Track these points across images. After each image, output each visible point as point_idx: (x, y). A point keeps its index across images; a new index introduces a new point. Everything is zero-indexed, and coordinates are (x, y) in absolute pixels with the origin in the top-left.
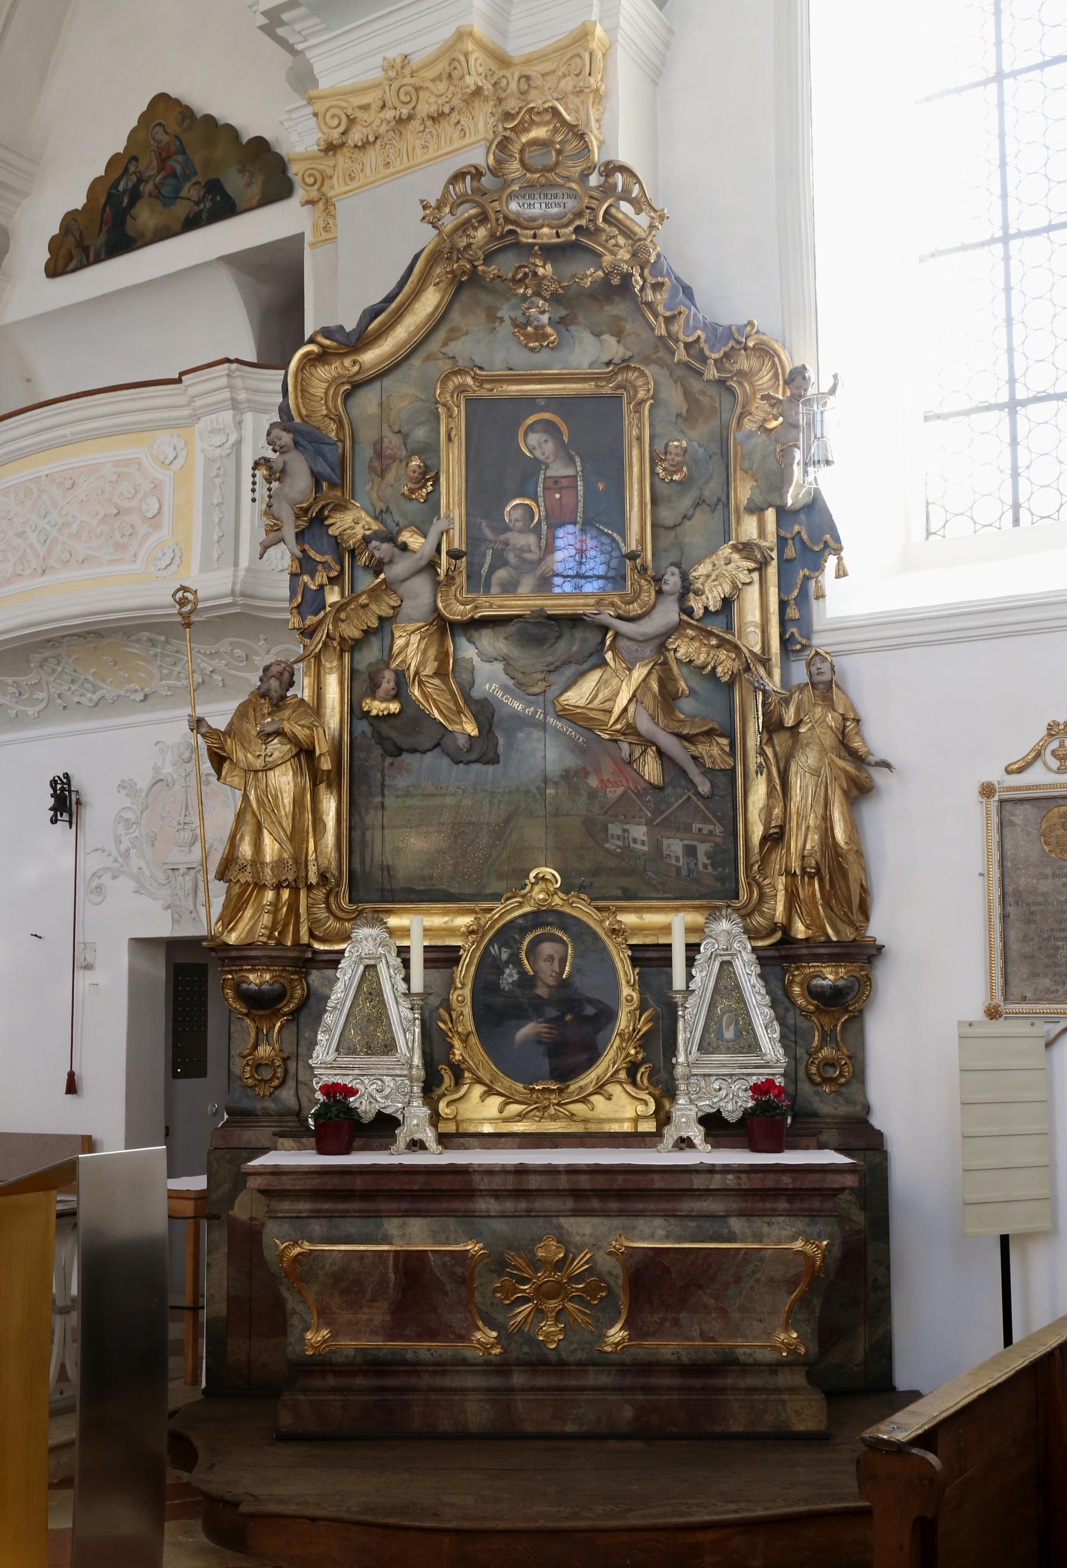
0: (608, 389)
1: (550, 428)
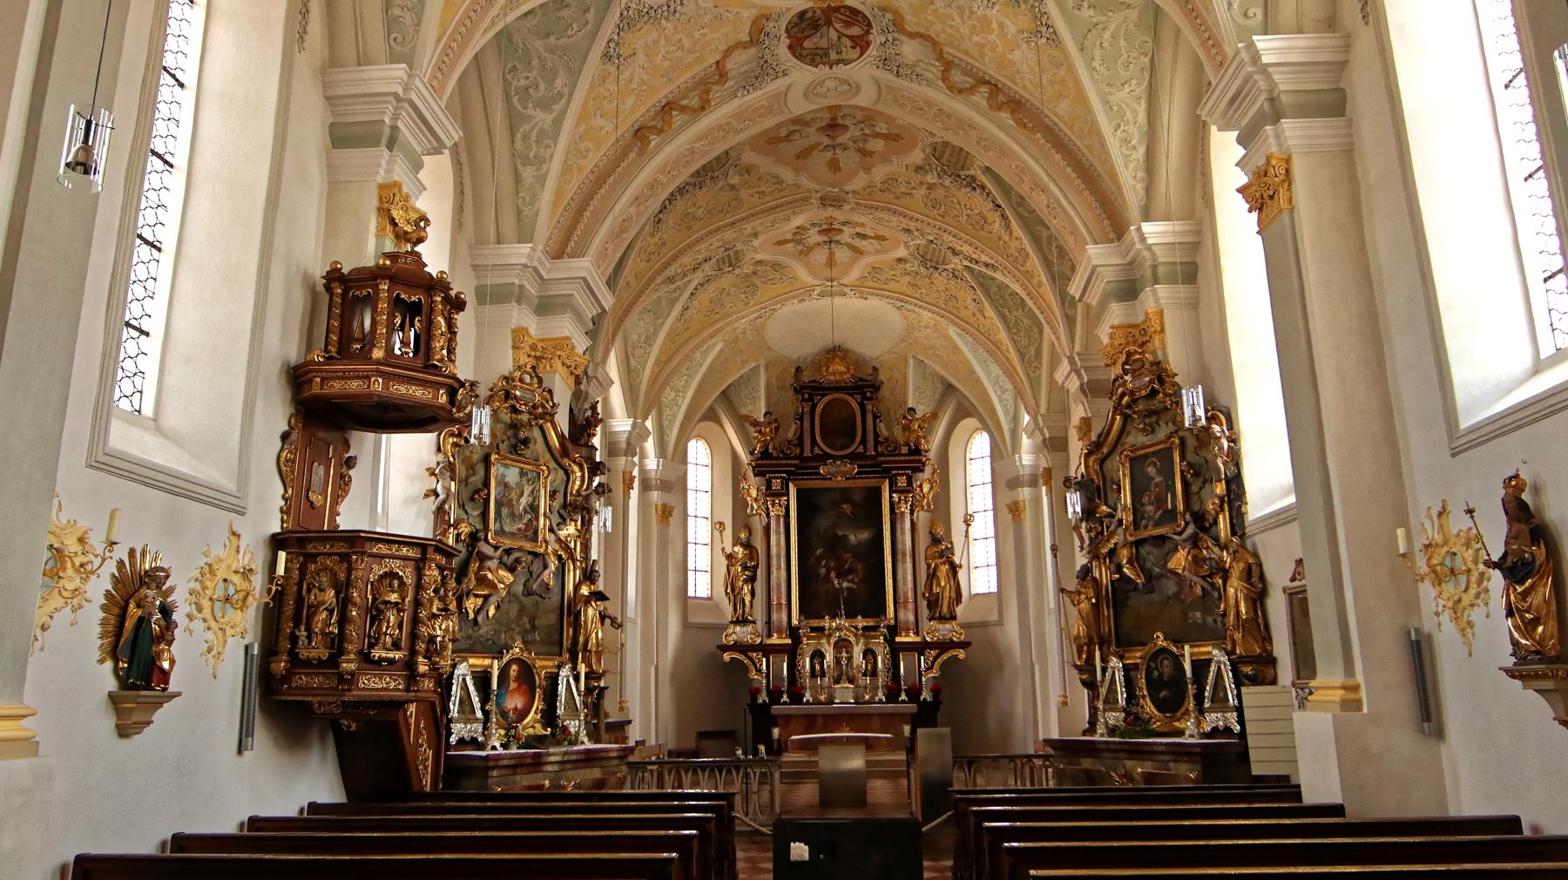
0: (1168, 445)
1: (1154, 464)
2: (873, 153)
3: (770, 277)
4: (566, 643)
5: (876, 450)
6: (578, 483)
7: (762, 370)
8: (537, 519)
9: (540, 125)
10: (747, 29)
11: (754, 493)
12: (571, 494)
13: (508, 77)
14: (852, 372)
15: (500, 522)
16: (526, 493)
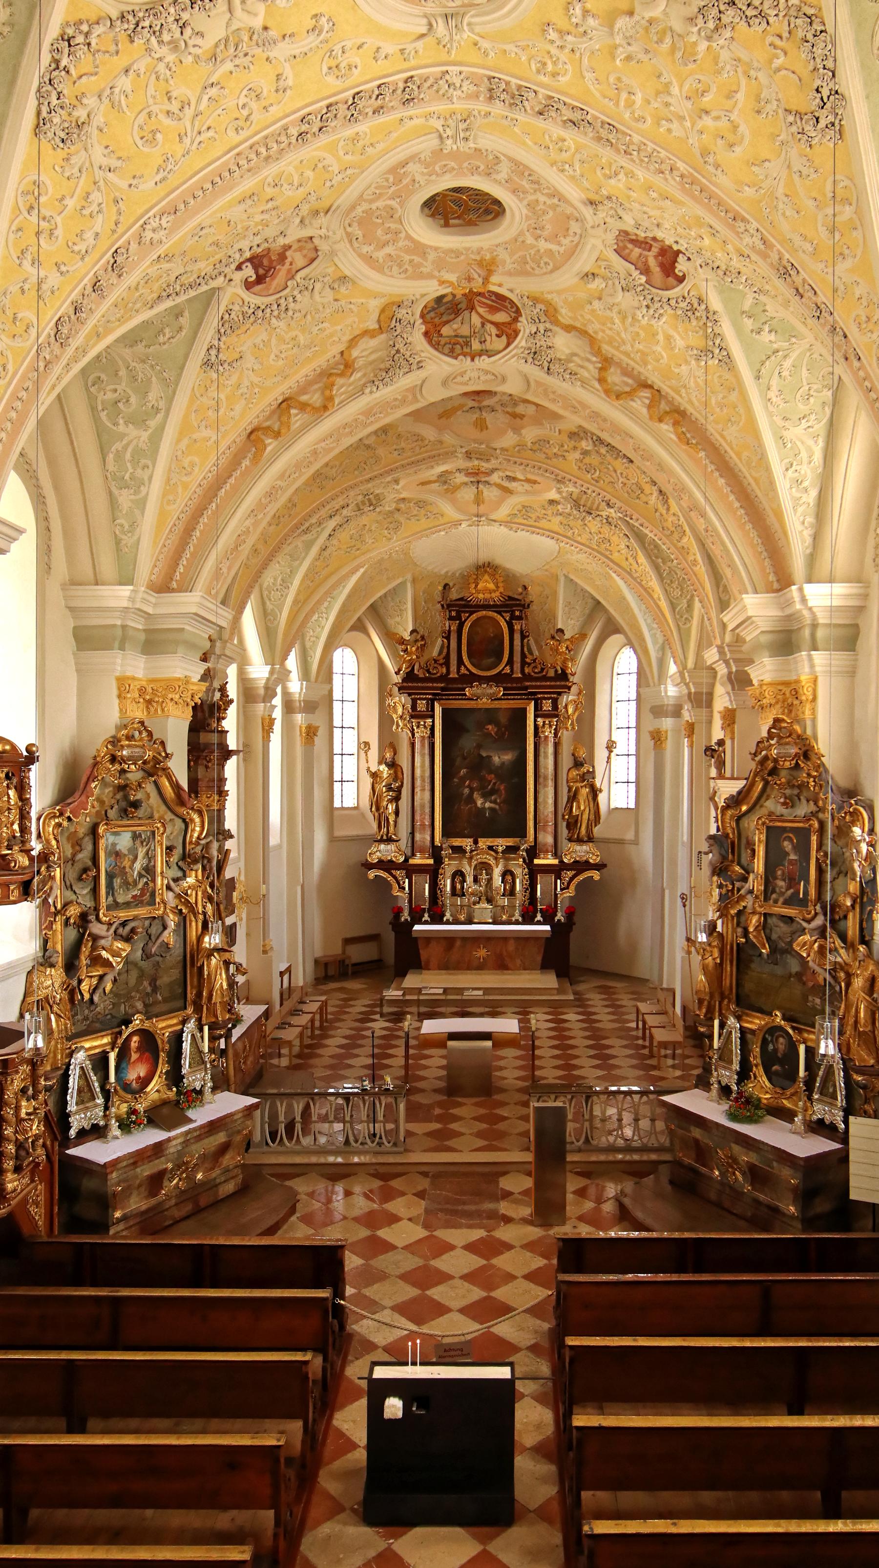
2: (524, 416)
3: (415, 512)
4: (191, 995)
5: (522, 672)
6: (198, 829)
7: (409, 585)
8: (154, 881)
10: (375, 316)
11: (400, 710)
12: (191, 842)
13: (92, 389)
14: (501, 590)
15: (113, 895)
16: (141, 855)
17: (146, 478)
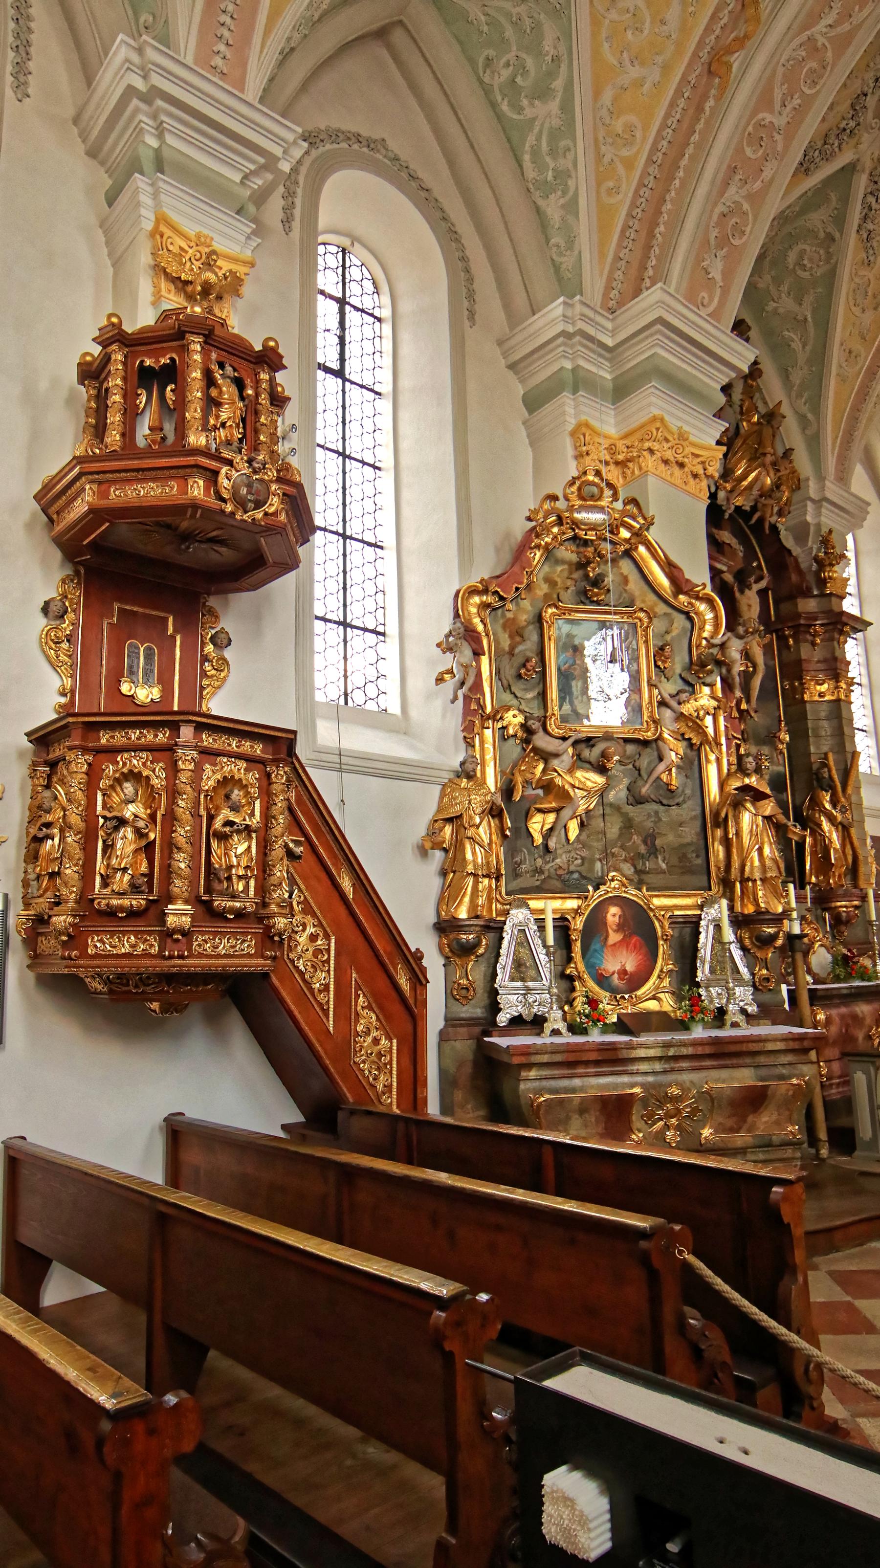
6: (709, 628)
9: (547, 125)
13: (487, 79)
15: (571, 703)
17: (570, 166)
